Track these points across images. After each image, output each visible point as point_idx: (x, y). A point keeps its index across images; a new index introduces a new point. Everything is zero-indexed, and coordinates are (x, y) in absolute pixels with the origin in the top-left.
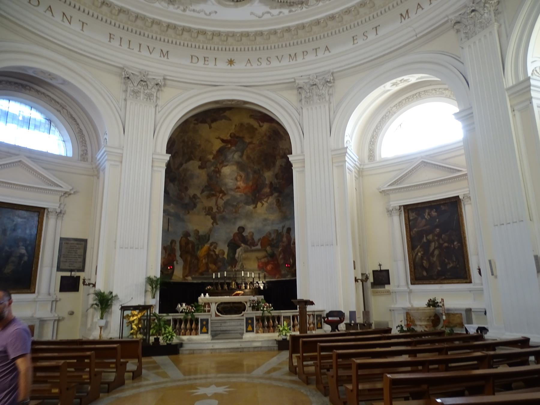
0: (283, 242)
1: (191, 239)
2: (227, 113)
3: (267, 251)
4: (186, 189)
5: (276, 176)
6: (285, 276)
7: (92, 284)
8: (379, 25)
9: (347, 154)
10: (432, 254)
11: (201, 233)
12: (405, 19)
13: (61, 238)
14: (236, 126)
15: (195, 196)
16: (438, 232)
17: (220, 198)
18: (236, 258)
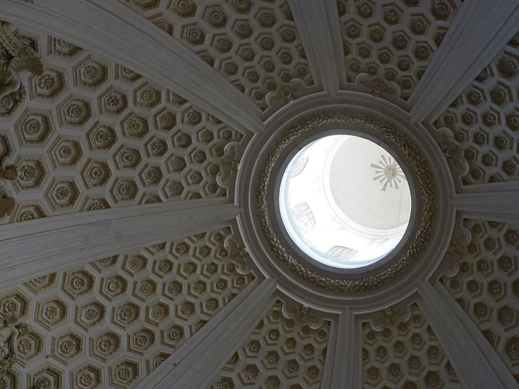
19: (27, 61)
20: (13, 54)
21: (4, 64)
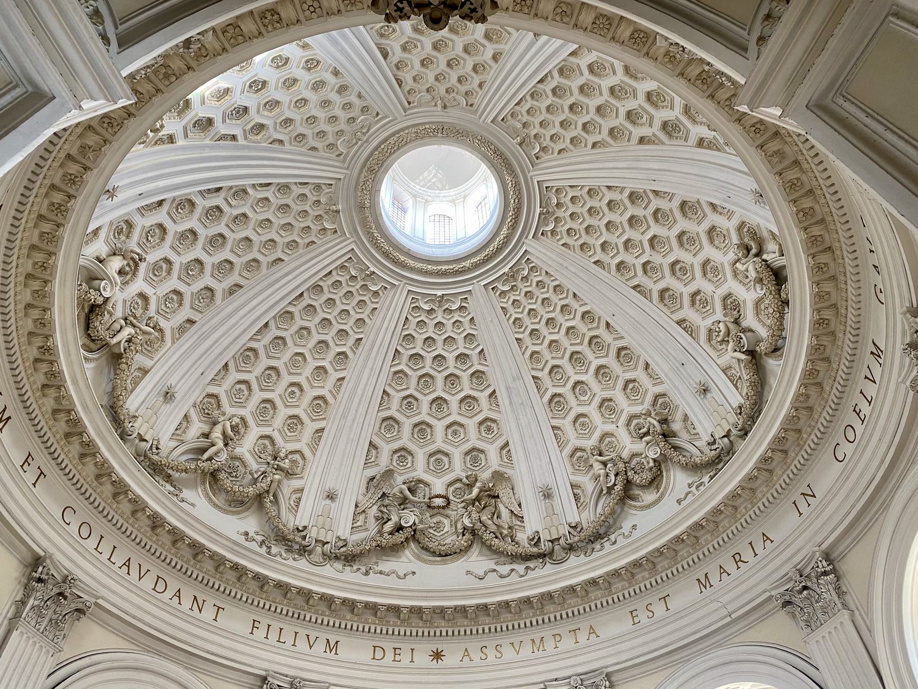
20: (381, 493)
21: (389, 500)
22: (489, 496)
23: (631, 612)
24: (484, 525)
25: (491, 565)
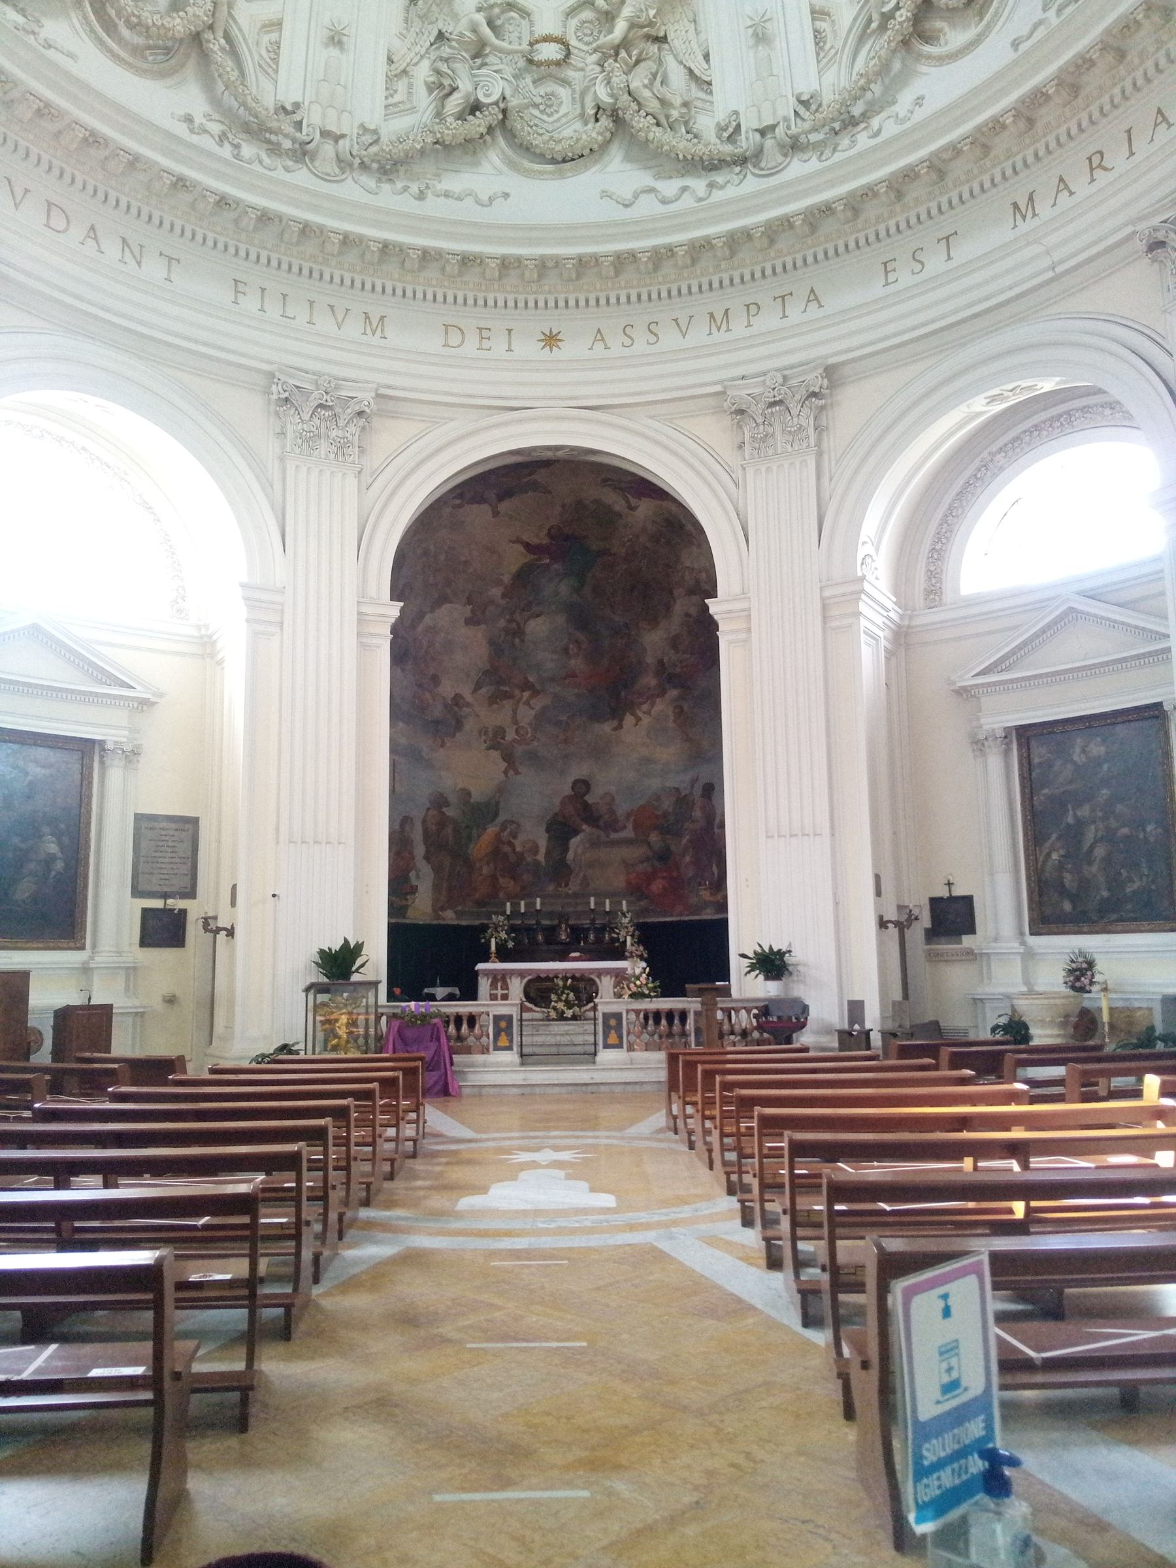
0: (693, 822)
1: (450, 812)
2: (541, 476)
3: (649, 844)
4: (435, 679)
5: (675, 642)
6: (699, 909)
7: (225, 929)
8: (956, 233)
9: (863, 596)
10: (1089, 857)
11: (476, 797)
12: (1024, 217)
13: (136, 814)
14: (563, 506)
15: (457, 700)
16: (1105, 797)
17: (524, 703)
18: (569, 862)
19: (441, 6)
20: (435, 32)
22: (648, 37)
23: (885, 264)
24: (635, 100)
25: (645, 179)
